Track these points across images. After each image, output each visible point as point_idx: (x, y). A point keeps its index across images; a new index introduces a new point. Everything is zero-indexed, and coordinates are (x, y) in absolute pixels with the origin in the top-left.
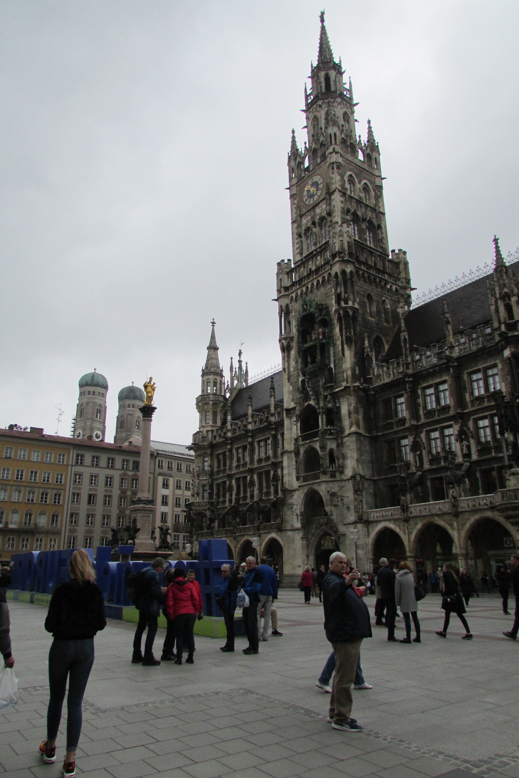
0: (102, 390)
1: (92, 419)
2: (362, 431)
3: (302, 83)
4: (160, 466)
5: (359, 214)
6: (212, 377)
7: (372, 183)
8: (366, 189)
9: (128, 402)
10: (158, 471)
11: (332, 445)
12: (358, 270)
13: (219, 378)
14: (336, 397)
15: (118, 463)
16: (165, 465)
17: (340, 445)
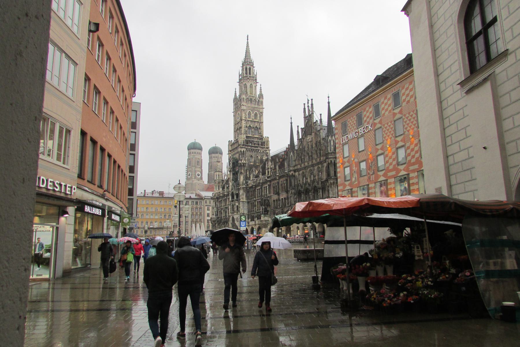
0: (199, 151)
1: (195, 166)
2: (244, 200)
3: (238, 69)
4: (206, 202)
5: (251, 126)
6: (218, 173)
7: (258, 111)
8: (256, 115)
9: (213, 155)
10: (205, 204)
11: (237, 204)
12: (247, 149)
13: (220, 173)
14: (239, 189)
15: (190, 203)
16: (208, 202)
17: (239, 204)
